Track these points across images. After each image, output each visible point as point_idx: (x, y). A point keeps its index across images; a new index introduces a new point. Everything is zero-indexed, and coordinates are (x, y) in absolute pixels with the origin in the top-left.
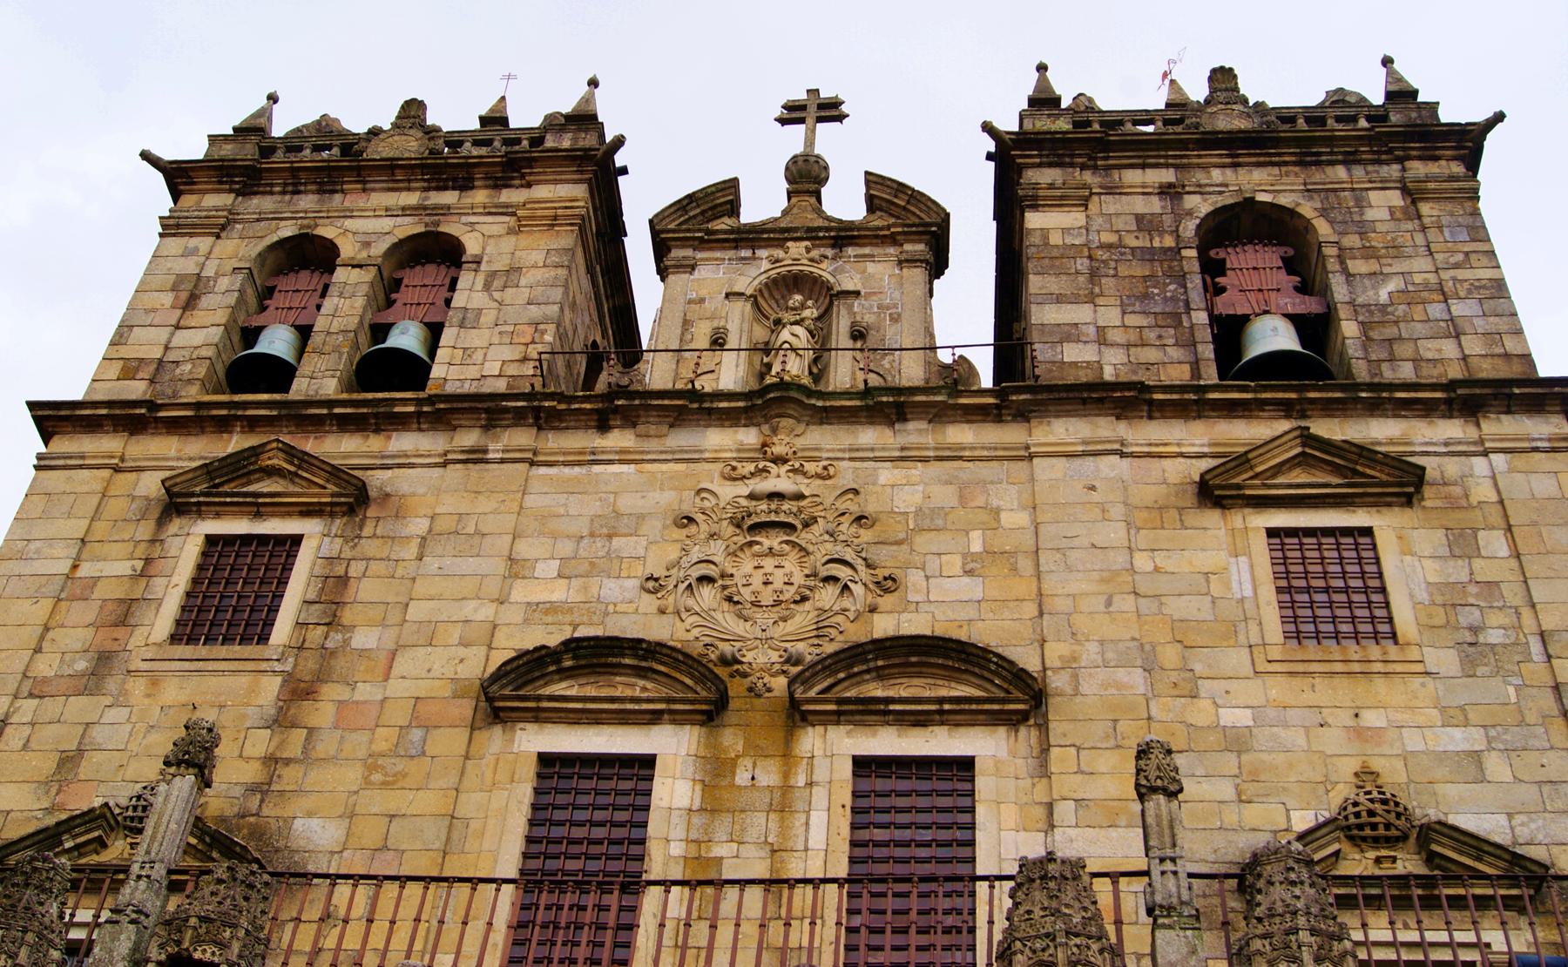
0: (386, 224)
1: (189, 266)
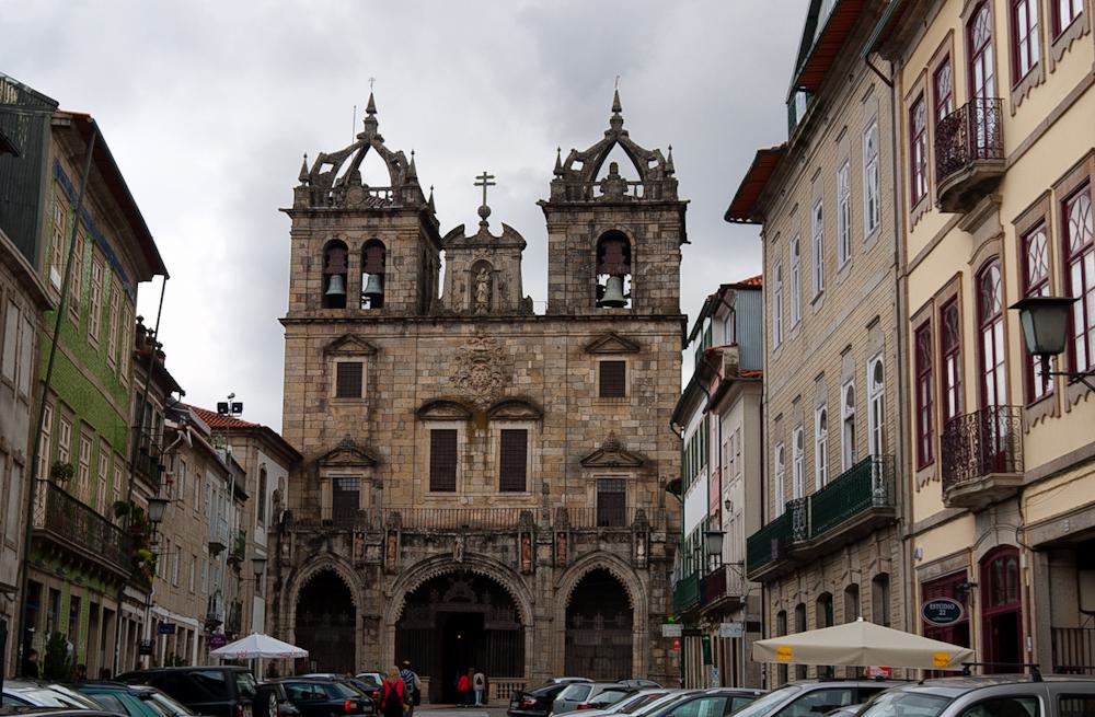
0: (358, 234)
1: (303, 253)
